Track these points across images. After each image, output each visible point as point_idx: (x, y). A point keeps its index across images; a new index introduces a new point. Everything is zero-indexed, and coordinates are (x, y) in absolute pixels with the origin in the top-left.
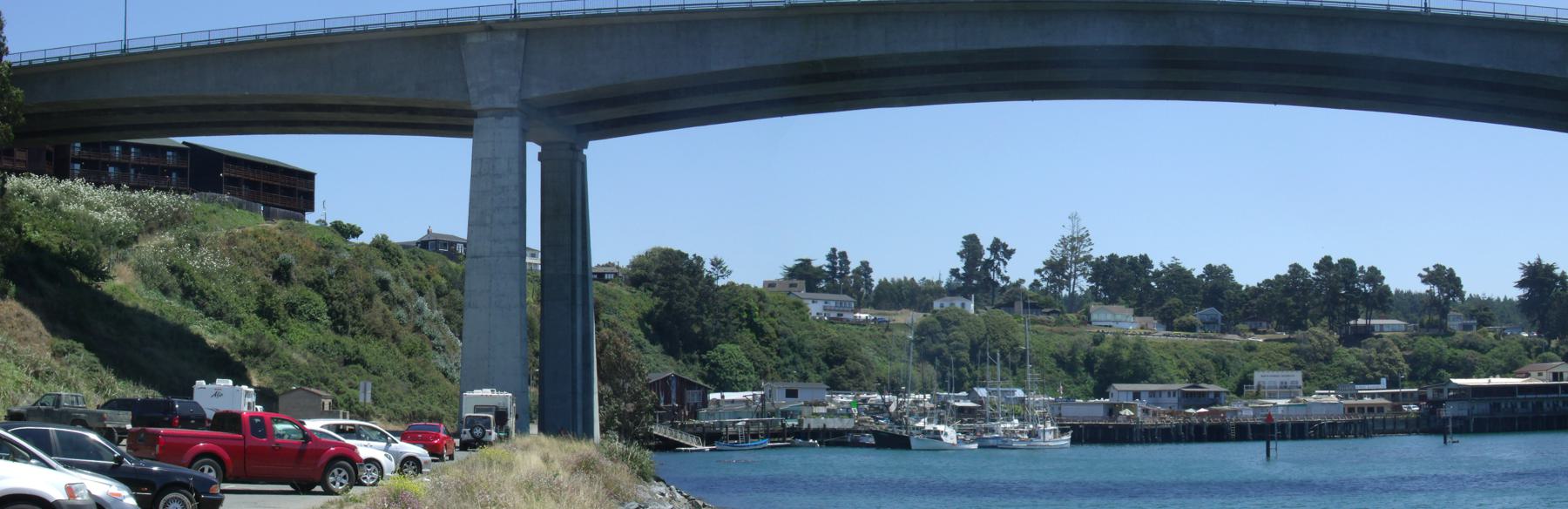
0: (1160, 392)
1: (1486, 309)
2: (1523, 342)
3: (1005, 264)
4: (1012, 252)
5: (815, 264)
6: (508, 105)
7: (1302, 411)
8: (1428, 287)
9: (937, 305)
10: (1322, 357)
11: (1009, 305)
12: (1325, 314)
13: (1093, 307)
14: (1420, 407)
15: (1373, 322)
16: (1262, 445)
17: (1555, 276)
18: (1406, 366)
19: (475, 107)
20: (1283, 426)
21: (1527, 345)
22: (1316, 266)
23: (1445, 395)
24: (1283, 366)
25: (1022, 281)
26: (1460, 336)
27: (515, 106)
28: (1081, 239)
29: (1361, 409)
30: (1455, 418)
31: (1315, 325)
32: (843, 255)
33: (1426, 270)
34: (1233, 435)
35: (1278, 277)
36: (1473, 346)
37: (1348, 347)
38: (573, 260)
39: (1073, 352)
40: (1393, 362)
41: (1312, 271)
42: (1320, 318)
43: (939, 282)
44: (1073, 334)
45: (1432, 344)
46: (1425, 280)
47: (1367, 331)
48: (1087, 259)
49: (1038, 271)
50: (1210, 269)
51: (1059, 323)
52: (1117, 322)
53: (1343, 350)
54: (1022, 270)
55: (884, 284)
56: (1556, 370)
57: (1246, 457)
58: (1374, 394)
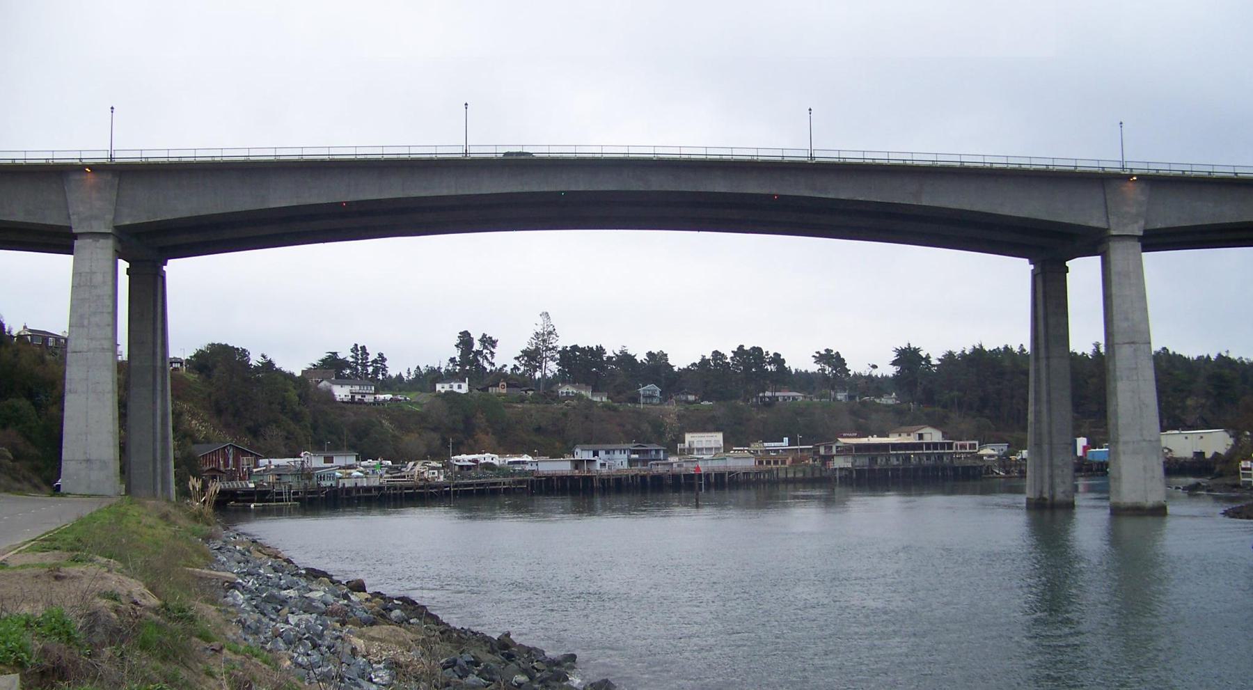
5: (341, 356)
15: (777, 394)
27: (110, 231)
28: (550, 333)
32: (363, 348)
33: (817, 353)
38: (154, 354)
49: (517, 358)
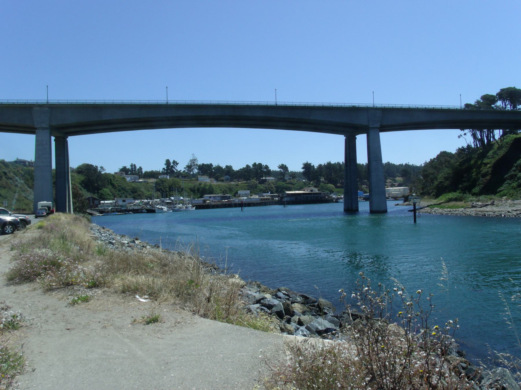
0: (216, 196)
1: (294, 174)
2: (304, 182)
3: (176, 166)
4: (178, 163)
5: (127, 168)
6: (46, 126)
7: (250, 200)
8: (280, 169)
9: (160, 177)
10: (254, 187)
11: (178, 177)
12: (255, 176)
13: (199, 176)
14: (278, 199)
15: (267, 178)
16: (241, 208)
17: (311, 166)
18: (275, 189)
19: (36, 126)
20: (245, 204)
21: (305, 183)
22: (252, 165)
23: (284, 195)
24: (245, 189)
25: (181, 170)
26: (288, 181)
27: (48, 127)
28: (195, 160)
29: (264, 199)
30: (286, 201)
31: (253, 179)
32: (135, 165)
33: (279, 165)
34: (234, 206)
35: (243, 168)
36: (291, 184)
37: (261, 184)
39: (194, 188)
40: (272, 188)
41: (251, 166)
42: (254, 177)
43: (160, 171)
44: (194, 183)
45: (281, 183)
46: (279, 168)
47: (265, 180)
48: (197, 165)
49: (185, 168)
50: (227, 167)
51: (190, 181)
52: (205, 180)
53: (260, 185)
54: (181, 168)
55: (146, 172)
56: (312, 189)
57: (236, 211)
58: (267, 196)
